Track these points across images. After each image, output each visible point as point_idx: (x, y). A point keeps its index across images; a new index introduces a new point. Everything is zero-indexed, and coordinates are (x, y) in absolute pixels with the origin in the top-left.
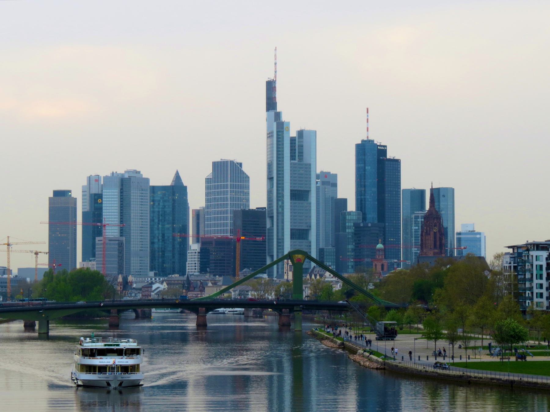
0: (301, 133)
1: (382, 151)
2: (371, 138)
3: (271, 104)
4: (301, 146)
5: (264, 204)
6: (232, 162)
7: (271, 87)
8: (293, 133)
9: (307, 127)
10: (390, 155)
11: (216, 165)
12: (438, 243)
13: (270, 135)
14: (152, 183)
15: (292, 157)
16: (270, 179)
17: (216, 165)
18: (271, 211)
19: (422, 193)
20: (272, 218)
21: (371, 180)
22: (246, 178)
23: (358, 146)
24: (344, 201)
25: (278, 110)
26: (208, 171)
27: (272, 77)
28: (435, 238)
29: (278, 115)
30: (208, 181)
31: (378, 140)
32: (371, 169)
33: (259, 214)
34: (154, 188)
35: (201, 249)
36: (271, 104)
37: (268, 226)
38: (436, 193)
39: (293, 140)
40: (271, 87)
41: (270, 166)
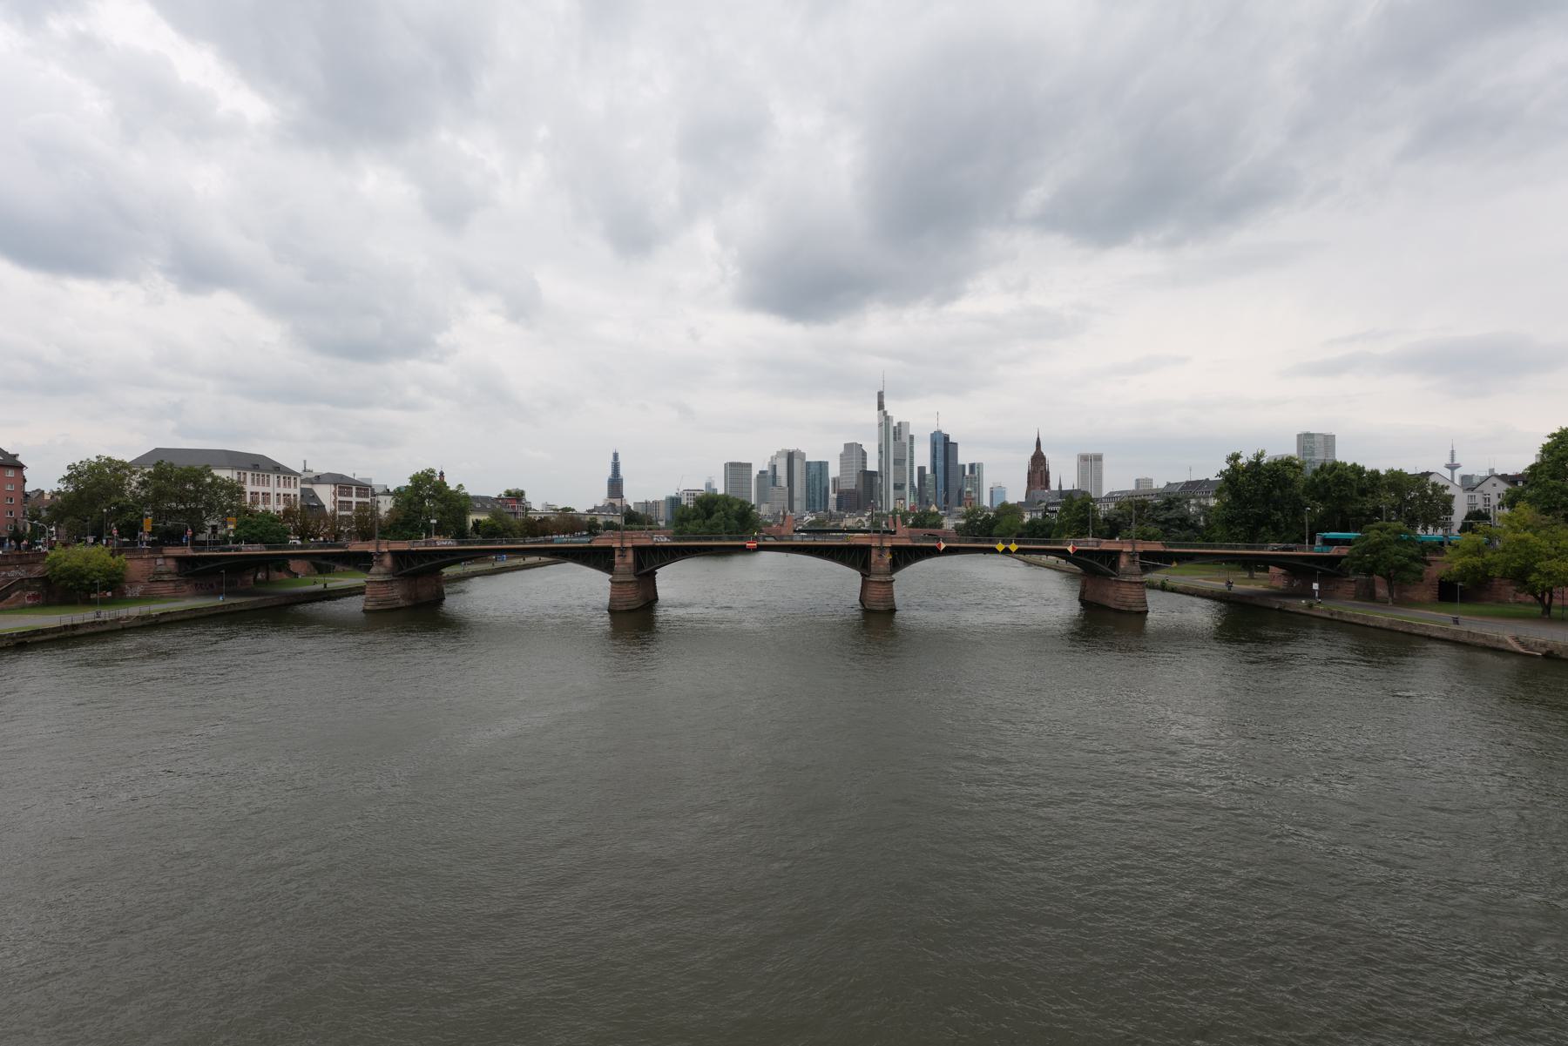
0: (899, 424)
1: (946, 438)
2: (940, 428)
3: (881, 406)
4: (900, 431)
5: (876, 469)
6: (856, 443)
7: (881, 395)
8: (895, 424)
9: (903, 420)
10: (950, 440)
11: (846, 446)
12: (1044, 480)
13: (880, 425)
14: (807, 460)
15: (895, 439)
16: (880, 452)
17: (846, 446)
18: (881, 471)
19: (964, 466)
20: (882, 477)
21: (940, 454)
22: (864, 454)
23: (932, 435)
24: (922, 469)
25: (885, 409)
26: (842, 450)
27: (882, 390)
28: (1042, 474)
29: (885, 413)
30: (841, 455)
31: (944, 432)
32: (940, 447)
33: (873, 474)
34: (808, 464)
35: (838, 496)
36: (881, 406)
37: (879, 482)
38: (972, 466)
39: (895, 428)
40: (881, 395)
41: (880, 446)
